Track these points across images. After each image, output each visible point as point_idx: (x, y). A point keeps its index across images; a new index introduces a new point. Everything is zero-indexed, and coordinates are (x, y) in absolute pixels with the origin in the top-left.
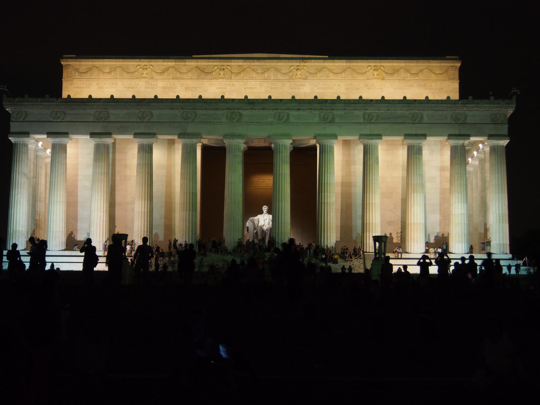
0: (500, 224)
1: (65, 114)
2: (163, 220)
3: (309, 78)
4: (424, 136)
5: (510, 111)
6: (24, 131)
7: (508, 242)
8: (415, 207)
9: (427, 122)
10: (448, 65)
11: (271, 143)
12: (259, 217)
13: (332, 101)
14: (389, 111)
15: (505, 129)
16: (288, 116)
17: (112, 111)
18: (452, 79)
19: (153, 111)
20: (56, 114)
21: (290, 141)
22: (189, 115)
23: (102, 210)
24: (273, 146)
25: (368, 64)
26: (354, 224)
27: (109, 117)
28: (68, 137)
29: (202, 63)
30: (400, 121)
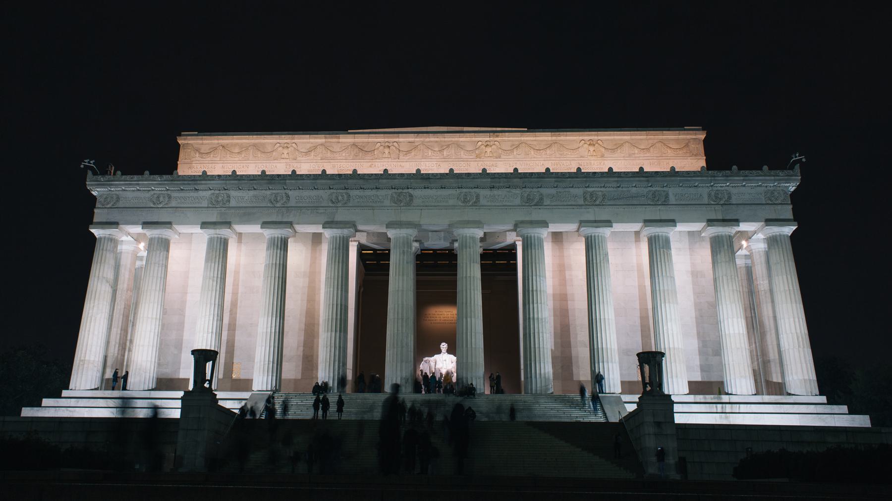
0: (801, 349)
1: (170, 197)
4: (672, 222)
5: (792, 189)
6: (113, 220)
7: (813, 376)
8: (669, 324)
13: (539, 175)
14: (620, 189)
15: (787, 212)
16: (478, 197)
17: (233, 193)
19: (290, 193)
20: (158, 197)
21: (480, 233)
22: (340, 198)
24: (456, 245)
30: (635, 202)
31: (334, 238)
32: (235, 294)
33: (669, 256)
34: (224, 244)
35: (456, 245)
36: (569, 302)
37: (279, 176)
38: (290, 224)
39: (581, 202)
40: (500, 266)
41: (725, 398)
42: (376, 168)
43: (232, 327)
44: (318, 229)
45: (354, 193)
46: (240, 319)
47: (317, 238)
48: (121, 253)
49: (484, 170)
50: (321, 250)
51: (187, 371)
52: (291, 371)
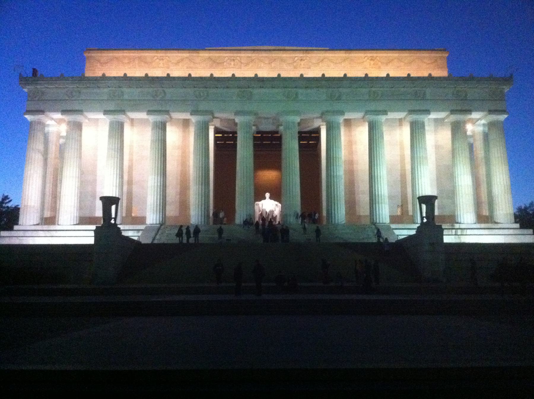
2: (178, 196)
3: (312, 68)
4: (427, 112)
9: (429, 98)
10: (438, 55)
11: (278, 126)
12: (263, 201)
14: (393, 89)
16: (297, 94)
17: (126, 90)
18: (442, 68)
21: (297, 119)
22: (202, 94)
23: (115, 185)
24: (281, 128)
25: (365, 55)
26: (357, 198)
27: (123, 95)
28: (82, 114)
29: (215, 55)
31: (198, 123)
32: (131, 160)
33: (424, 134)
34: (121, 126)
35: (281, 128)
36: (355, 166)
37: (157, 78)
38: (167, 112)
39: (367, 97)
40: (309, 141)
41: (457, 226)
42: (228, 74)
43: (130, 183)
44: (186, 116)
45: (212, 91)
46: (136, 177)
47: (186, 123)
48: (48, 133)
49: (302, 75)
50: (189, 131)
51: (99, 213)
52: (172, 211)
